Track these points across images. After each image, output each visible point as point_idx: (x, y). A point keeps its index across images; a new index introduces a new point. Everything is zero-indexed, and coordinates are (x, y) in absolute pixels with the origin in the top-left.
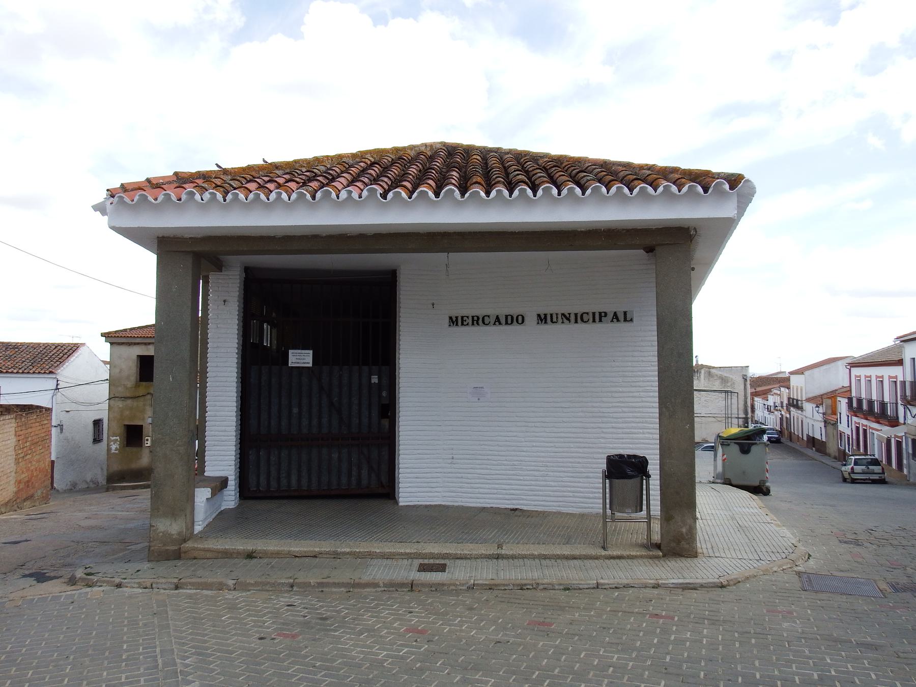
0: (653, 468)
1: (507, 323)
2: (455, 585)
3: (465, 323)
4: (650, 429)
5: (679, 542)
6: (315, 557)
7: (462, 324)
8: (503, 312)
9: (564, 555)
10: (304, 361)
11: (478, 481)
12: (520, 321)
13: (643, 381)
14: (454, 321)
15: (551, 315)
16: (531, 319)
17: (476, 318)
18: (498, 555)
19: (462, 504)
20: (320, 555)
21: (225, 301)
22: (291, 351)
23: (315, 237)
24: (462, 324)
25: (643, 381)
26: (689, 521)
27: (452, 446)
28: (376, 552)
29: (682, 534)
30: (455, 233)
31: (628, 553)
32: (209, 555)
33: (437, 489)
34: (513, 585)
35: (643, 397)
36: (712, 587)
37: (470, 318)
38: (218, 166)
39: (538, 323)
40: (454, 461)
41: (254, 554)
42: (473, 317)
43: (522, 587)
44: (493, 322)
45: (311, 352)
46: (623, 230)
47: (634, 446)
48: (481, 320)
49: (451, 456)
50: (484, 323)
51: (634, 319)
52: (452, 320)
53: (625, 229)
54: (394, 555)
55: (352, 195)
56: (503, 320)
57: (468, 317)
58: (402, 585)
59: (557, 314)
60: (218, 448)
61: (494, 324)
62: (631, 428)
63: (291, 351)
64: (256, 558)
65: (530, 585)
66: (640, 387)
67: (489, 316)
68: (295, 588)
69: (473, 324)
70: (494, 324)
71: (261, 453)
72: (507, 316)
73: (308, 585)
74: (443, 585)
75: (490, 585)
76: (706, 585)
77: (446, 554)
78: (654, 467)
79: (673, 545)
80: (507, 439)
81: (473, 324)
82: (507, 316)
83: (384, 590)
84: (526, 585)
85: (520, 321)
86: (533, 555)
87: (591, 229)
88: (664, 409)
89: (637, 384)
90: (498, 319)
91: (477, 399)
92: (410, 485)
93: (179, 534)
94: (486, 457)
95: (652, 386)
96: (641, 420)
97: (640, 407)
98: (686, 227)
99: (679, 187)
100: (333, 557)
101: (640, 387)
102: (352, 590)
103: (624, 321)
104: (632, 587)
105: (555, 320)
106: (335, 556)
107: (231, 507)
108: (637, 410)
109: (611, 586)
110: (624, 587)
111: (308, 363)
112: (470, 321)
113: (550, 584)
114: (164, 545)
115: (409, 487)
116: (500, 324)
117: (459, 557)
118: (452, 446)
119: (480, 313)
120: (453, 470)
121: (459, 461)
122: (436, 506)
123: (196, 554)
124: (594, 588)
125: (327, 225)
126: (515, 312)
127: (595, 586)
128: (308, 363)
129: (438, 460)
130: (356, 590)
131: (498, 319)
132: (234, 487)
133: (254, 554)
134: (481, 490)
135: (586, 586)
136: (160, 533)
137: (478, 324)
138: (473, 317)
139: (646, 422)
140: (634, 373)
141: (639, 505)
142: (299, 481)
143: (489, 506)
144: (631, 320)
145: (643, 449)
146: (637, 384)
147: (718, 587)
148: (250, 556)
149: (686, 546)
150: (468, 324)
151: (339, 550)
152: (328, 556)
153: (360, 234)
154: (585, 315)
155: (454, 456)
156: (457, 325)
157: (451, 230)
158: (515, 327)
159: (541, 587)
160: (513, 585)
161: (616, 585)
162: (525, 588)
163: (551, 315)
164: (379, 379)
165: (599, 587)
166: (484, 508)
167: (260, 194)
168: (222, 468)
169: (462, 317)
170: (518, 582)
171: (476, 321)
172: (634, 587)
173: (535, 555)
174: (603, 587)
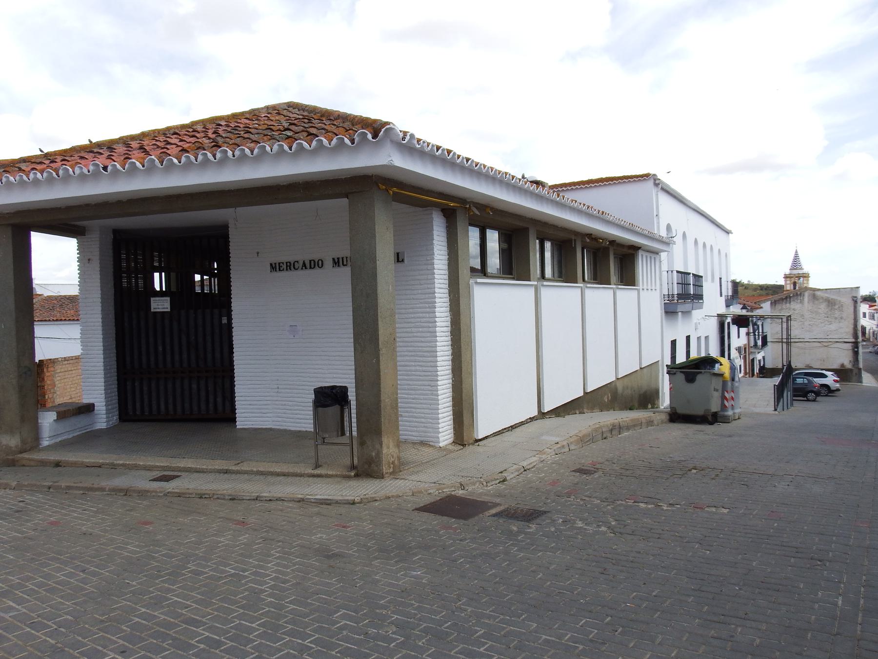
0: (423, 398)
1: (311, 268)
2: (156, 492)
3: (281, 269)
4: (419, 362)
5: (370, 464)
6: (100, 467)
7: (280, 270)
8: (307, 258)
9: (276, 472)
10: (164, 307)
11: (296, 408)
12: (320, 266)
13: (414, 318)
14: (274, 267)
15: (343, 258)
16: (328, 263)
17: (288, 264)
18: (227, 470)
19: (286, 428)
20: (103, 466)
21: (89, 260)
22: (152, 299)
23: (87, 205)
24: (280, 270)
25: (414, 318)
26: (377, 446)
27: (278, 378)
28: (140, 465)
29: (372, 458)
30: (185, 194)
31: (326, 473)
32: (32, 463)
33: (268, 415)
34: (196, 494)
35: (414, 333)
36: (345, 504)
37: (285, 264)
38: (41, 151)
39: (333, 267)
40: (280, 390)
41: (60, 464)
42: (287, 263)
43: (201, 496)
44: (301, 267)
45: (168, 299)
46: (318, 181)
47: (408, 377)
48: (292, 265)
49: (276, 386)
50: (294, 268)
51: (406, 261)
52: (272, 267)
53: (319, 181)
54: (153, 468)
55: (83, 170)
56: (308, 265)
57: (283, 263)
58: (121, 490)
59: (347, 258)
60: (91, 380)
61: (302, 269)
62: (406, 362)
63: (152, 299)
64: (61, 466)
65: (207, 494)
66: (411, 323)
67: (298, 262)
68: (51, 490)
69: (287, 270)
70: (302, 269)
71: (136, 384)
72: (310, 261)
73: (60, 487)
74: (148, 491)
75: (179, 493)
76: (340, 501)
77: (189, 468)
78: (424, 397)
79: (366, 466)
80: (316, 371)
81: (287, 270)
82: (310, 261)
83: (108, 494)
84: (204, 494)
85: (320, 266)
86: (252, 471)
87: (291, 183)
88: (357, 345)
89: (410, 320)
90: (304, 265)
91: (293, 336)
92: (244, 411)
93: (16, 446)
94: (301, 387)
95: (421, 323)
96: (413, 354)
97: (412, 342)
98: (371, 175)
99: (142, 161)
100: (111, 467)
101: (411, 323)
102: (87, 492)
103: (397, 262)
104: (283, 500)
105: (345, 263)
106: (113, 467)
107: (103, 428)
108: (409, 344)
109: (266, 498)
110: (277, 499)
111: (167, 308)
112: (285, 266)
113: (222, 495)
114: (7, 455)
115: (244, 413)
116: (306, 268)
117: (198, 470)
118: (278, 378)
119: (291, 259)
120: (279, 399)
121: (283, 390)
122: (266, 429)
123: (24, 462)
124: (254, 500)
125: (239, 180)
126: (316, 257)
127: (255, 498)
128: (167, 308)
129: (268, 390)
130: (90, 493)
131: (304, 265)
132: (105, 411)
133: (60, 464)
134: (299, 416)
135: (248, 498)
136: (4, 445)
137: (290, 270)
138: (287, 263)
139: (417, 356)
140: (407, 310)
141: (340, 430)
142: (167, 408)
143: (304, 430)
144: (403, 261)
145: (416, 381)
146: (410, 320)
147: (350, 504)
148: (58, 464)
149: (376, 468)
150: (283, 270)
151: (115, 462)
152: (108, 466)
153: (118, 201)
154: (296, 263)
155: (279, 386)
156: (276, 271)
157: (182, 192)
158: (317, 271)
159: (215, 497)
160: (196, 494)
161: (270, 498)
162: (204, 497)
163: (343, 258)
164: (221, 321)
165: (258, 499)
166: (300, 431)
167: (22, 176)
168: (95, 396)
169: (279, 263)
170: (199, 492)
171: (290, 266)
172: (284, 500)
173: (254, 471)
174: (261, 499)
